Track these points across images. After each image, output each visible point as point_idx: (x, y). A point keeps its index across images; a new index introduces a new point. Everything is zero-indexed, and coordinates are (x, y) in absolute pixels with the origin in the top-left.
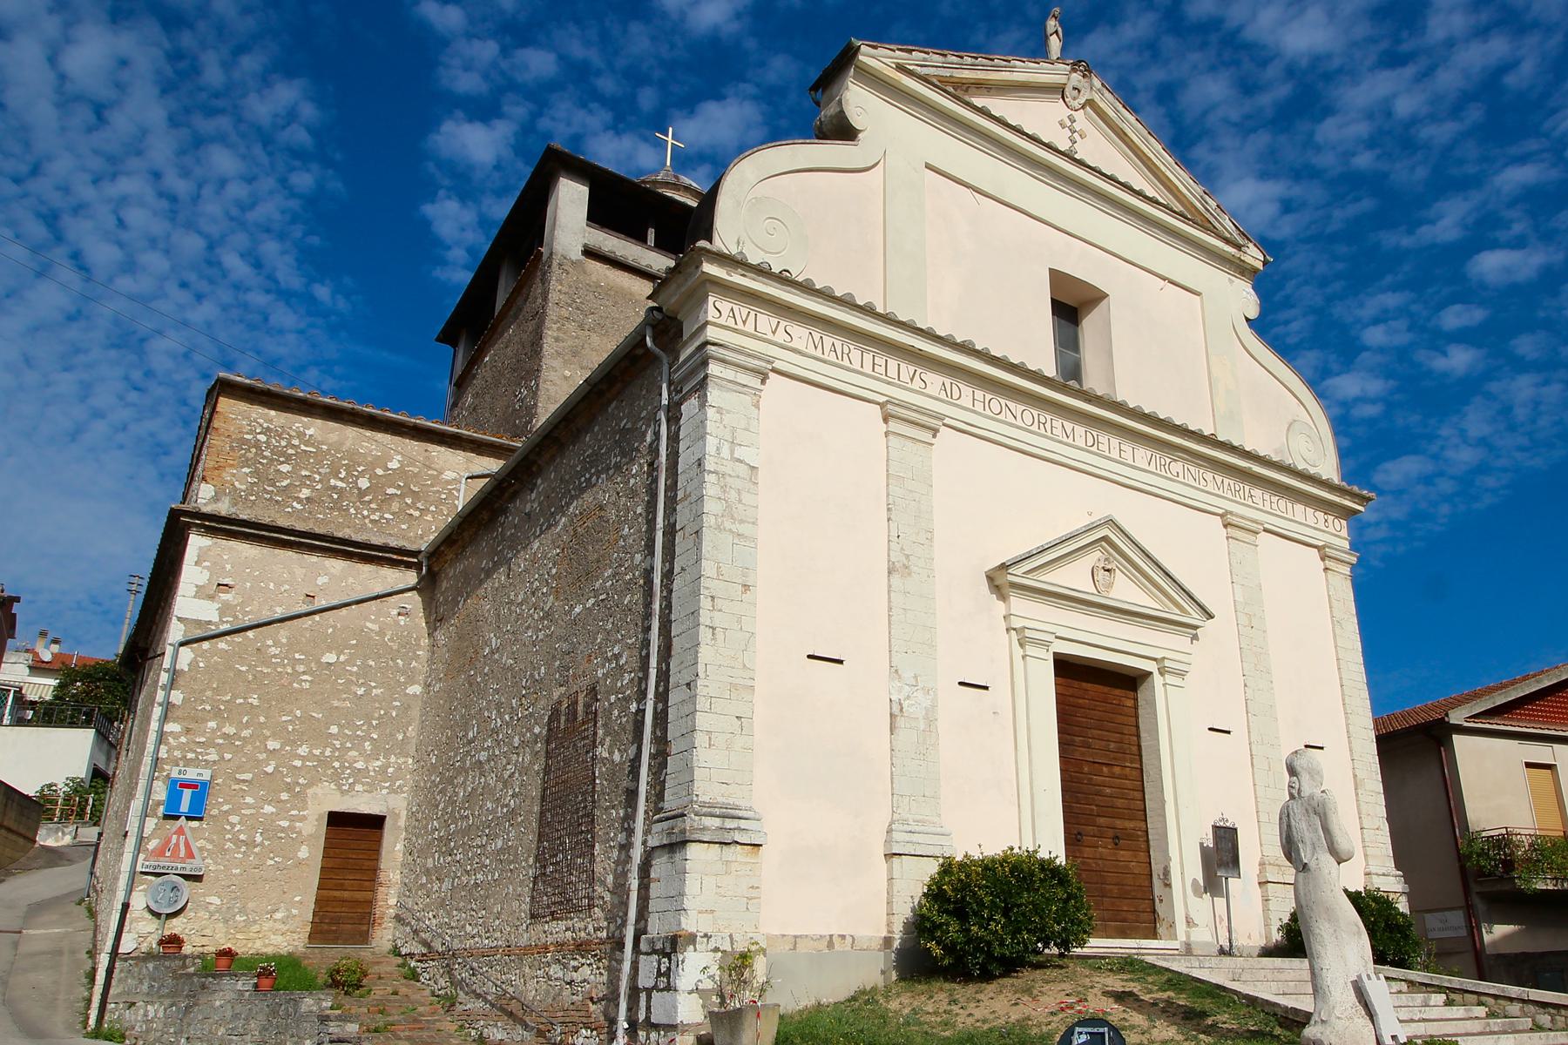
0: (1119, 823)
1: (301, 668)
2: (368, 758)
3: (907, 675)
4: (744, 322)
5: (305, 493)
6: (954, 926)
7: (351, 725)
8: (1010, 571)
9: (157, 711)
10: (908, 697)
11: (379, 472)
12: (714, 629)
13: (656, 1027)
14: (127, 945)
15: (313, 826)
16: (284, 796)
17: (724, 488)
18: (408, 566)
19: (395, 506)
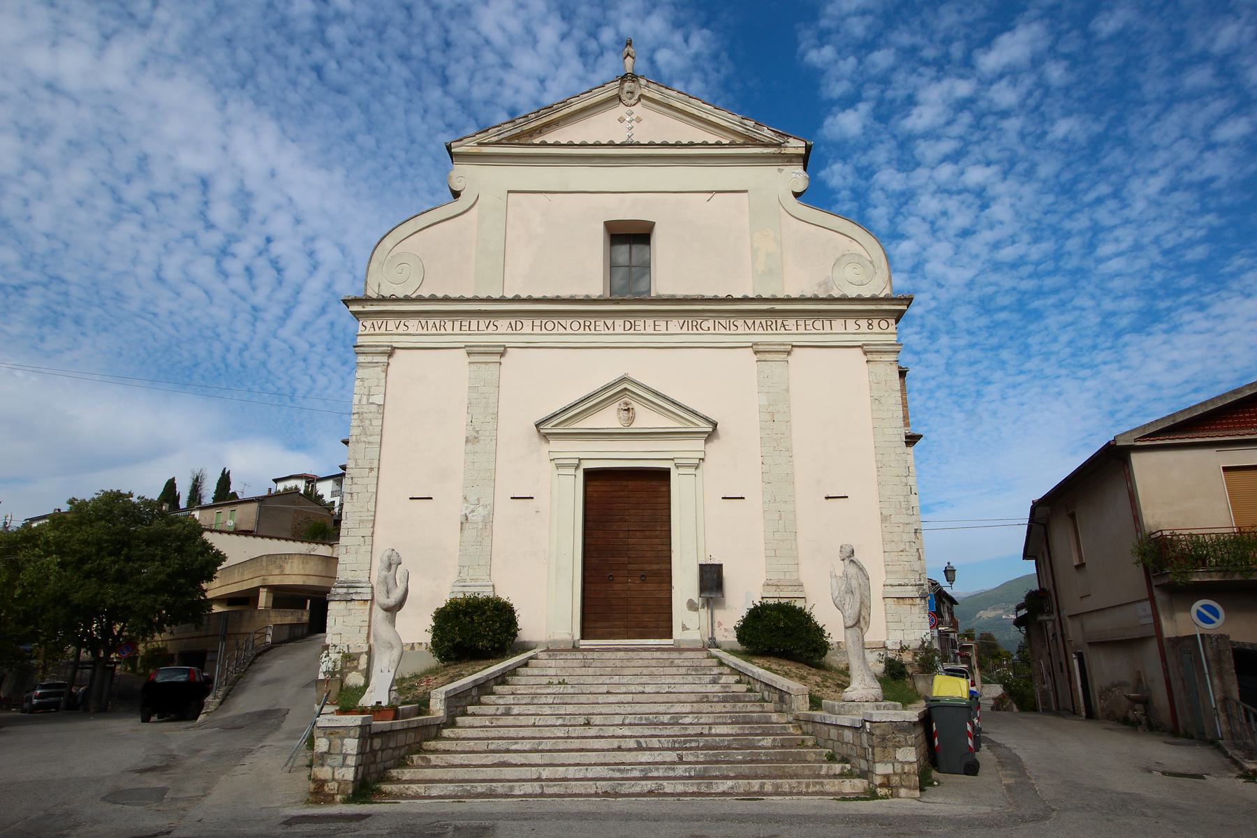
0: (646, 567)
3: (473, 499)
4: (379, 328)
8: (541, 427)
10: (473, 511)
12: (352, 494)
17: (362, 421)
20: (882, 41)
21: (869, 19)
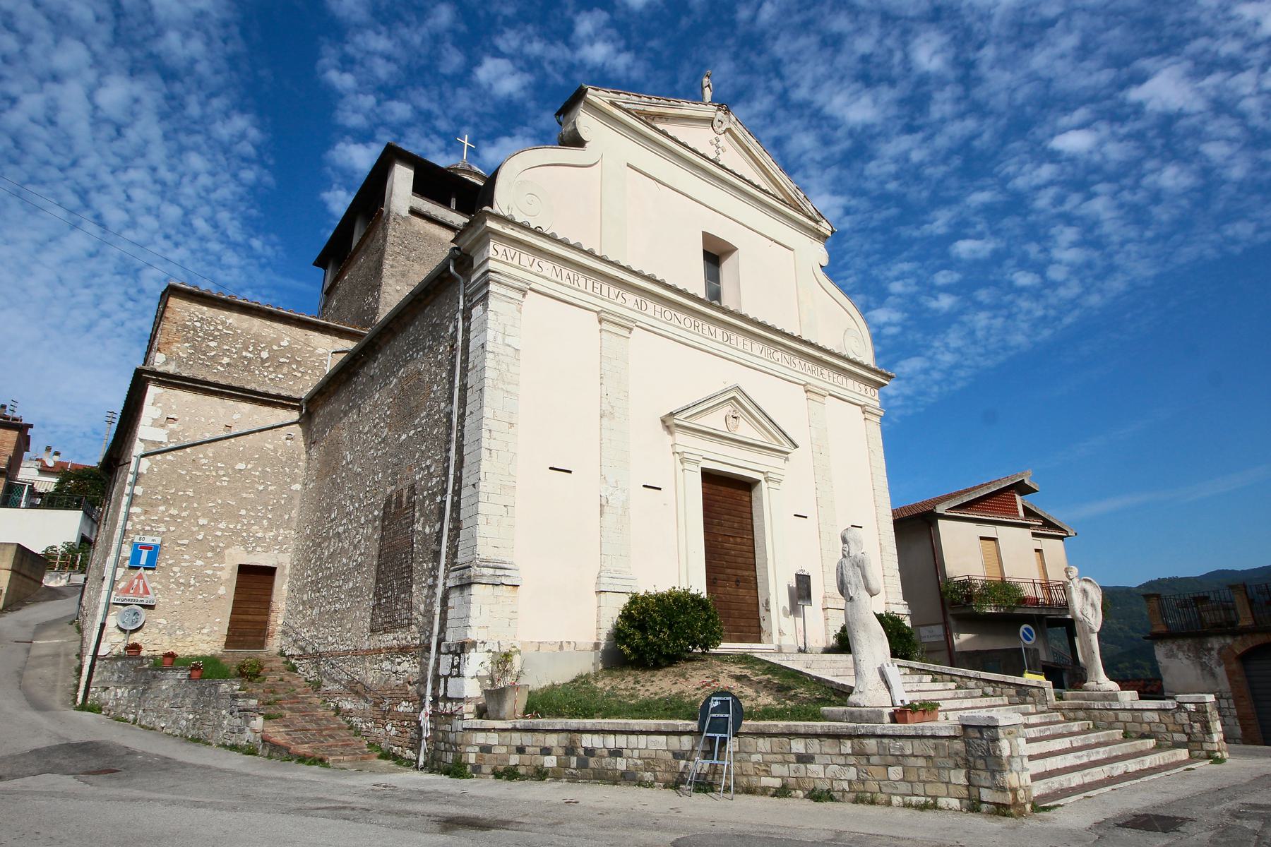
0: (739, 572)
1: (222, 473)
2: (265, 530)
4: (512, 259)
5: (226, 360)
6: (638, 636)
7: (254, 509)
9: (125, 500)
10: (612, 494)
11: (275, 348)
13: (451, 700)
14: (103, 650)
15: (228, 575)
16: (210, 554)
17: (498, 362)
18: (294, 408)
19: (285, 370)
20: (402, 94)
21: (393, 67)
